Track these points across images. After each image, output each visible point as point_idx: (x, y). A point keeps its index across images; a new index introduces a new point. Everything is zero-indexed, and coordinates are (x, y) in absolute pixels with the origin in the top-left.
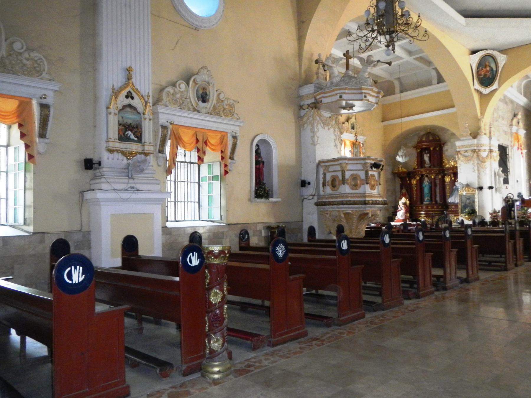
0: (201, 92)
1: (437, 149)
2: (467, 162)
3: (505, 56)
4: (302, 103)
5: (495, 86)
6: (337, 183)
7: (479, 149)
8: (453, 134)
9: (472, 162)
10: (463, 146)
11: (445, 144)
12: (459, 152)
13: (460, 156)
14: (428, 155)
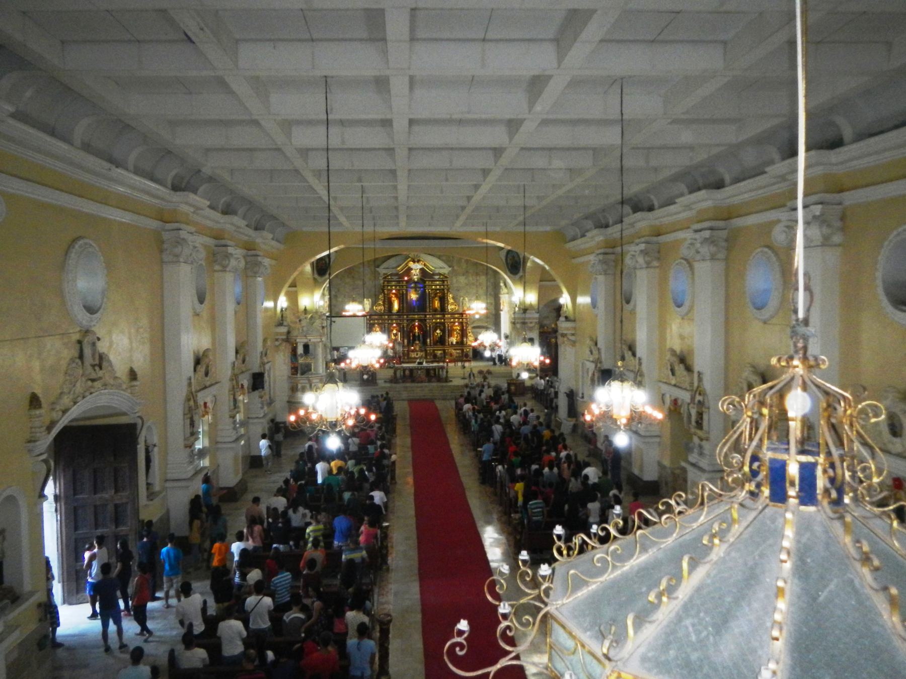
4: (277, 337)
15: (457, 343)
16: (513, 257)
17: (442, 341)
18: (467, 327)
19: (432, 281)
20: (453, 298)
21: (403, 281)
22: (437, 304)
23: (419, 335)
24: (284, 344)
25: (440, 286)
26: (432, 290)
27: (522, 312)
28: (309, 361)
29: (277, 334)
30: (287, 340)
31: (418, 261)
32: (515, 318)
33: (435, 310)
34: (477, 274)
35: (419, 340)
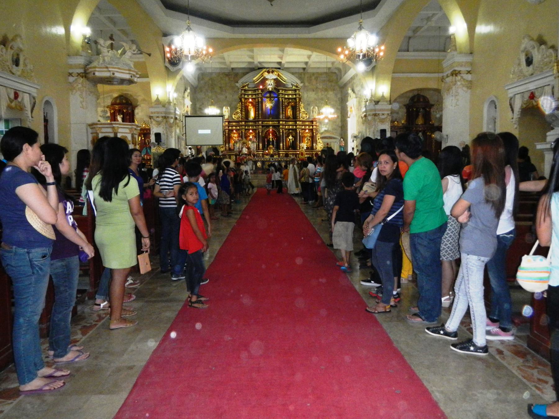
0: (15, 57)
4: (71, 71)
10: (154, 113)
11: (137, 108)
12: (152, 117)
14: (122, 116)
17: (294, 146)
18: (316, 135)
19: (285, 90)
21: (258, 90)
22: (289, 112)
23: (273, 141)
25: (292, 95)
26: (285, 99)
27: (374, 103)
29: (71, 66)
31: (273, 72)
33: (289, 118)
34: (326, 90)
35: (273, 145)
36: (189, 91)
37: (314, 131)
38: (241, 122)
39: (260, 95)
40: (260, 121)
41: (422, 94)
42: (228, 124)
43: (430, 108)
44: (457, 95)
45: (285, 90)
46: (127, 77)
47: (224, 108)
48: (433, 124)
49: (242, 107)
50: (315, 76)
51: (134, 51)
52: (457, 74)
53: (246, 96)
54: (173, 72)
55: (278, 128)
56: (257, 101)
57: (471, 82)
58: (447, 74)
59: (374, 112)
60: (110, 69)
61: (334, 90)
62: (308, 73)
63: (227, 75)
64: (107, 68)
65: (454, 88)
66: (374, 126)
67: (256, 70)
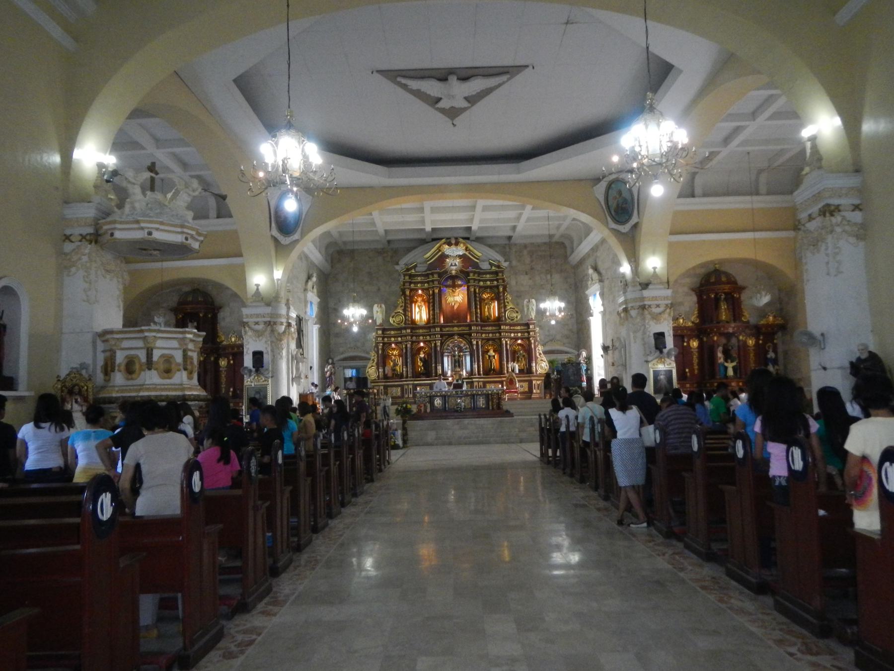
1: (209, 316)
2: (257, 339)
3: (311, 197)
4: (68, 232)
5: (296, 236)
6: (137, 366)
7: (275, 320)
8: (235, 296)
9: (264, 340)
10: (251, 316)
12: (247, 323)
13: (247, 329)
15: (521, 371)
16: (620, 193)
19: (479, 274)
20: (513, 303)
24: (88, 248)
25: (491, 281)
26: (480, 287)
27: (639, 288)
28: (261, 381)
30: (95, 238)
31: (457, 244)
32: (626, 302)
34: (549, 272)
36: (314, 279)
37: (533, 341)
38: (405, 328)
39: (436, 283)
40: (437, 326)
41: (723, 269)
42: (383, 333)
43: (740, 293)
44: (837, 254)
45: (479, 274)
46: (178, 239)
47: (376, 306)
48: (748, 322)
49: (405, 303)
50: (528, 249)
51: (194, 191)
52: (834, 211)
53: (412, 285)
54: (287, 245)
55: (467, 337)
56: (431, 292)
57: (863, 226)
58: (810, 215)
59: (641, 304)
60: (143, 225)
61: (561, 271)
62: (515, 245)
63: (380, 252)
64: (138, 222)
65: (830, 239)
66: (642, 328)
67: (427, 242)
